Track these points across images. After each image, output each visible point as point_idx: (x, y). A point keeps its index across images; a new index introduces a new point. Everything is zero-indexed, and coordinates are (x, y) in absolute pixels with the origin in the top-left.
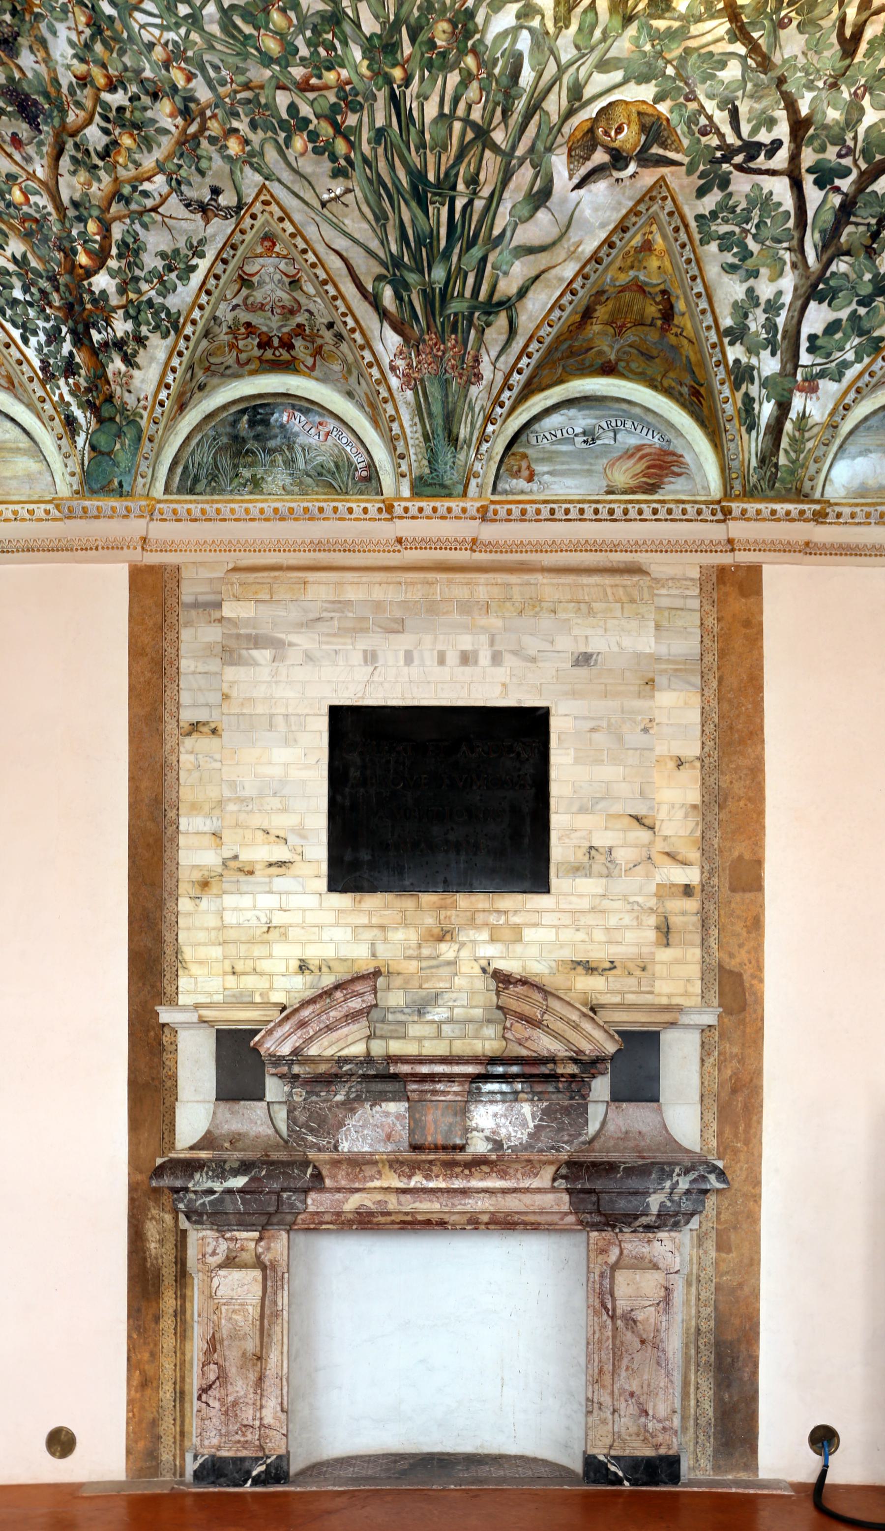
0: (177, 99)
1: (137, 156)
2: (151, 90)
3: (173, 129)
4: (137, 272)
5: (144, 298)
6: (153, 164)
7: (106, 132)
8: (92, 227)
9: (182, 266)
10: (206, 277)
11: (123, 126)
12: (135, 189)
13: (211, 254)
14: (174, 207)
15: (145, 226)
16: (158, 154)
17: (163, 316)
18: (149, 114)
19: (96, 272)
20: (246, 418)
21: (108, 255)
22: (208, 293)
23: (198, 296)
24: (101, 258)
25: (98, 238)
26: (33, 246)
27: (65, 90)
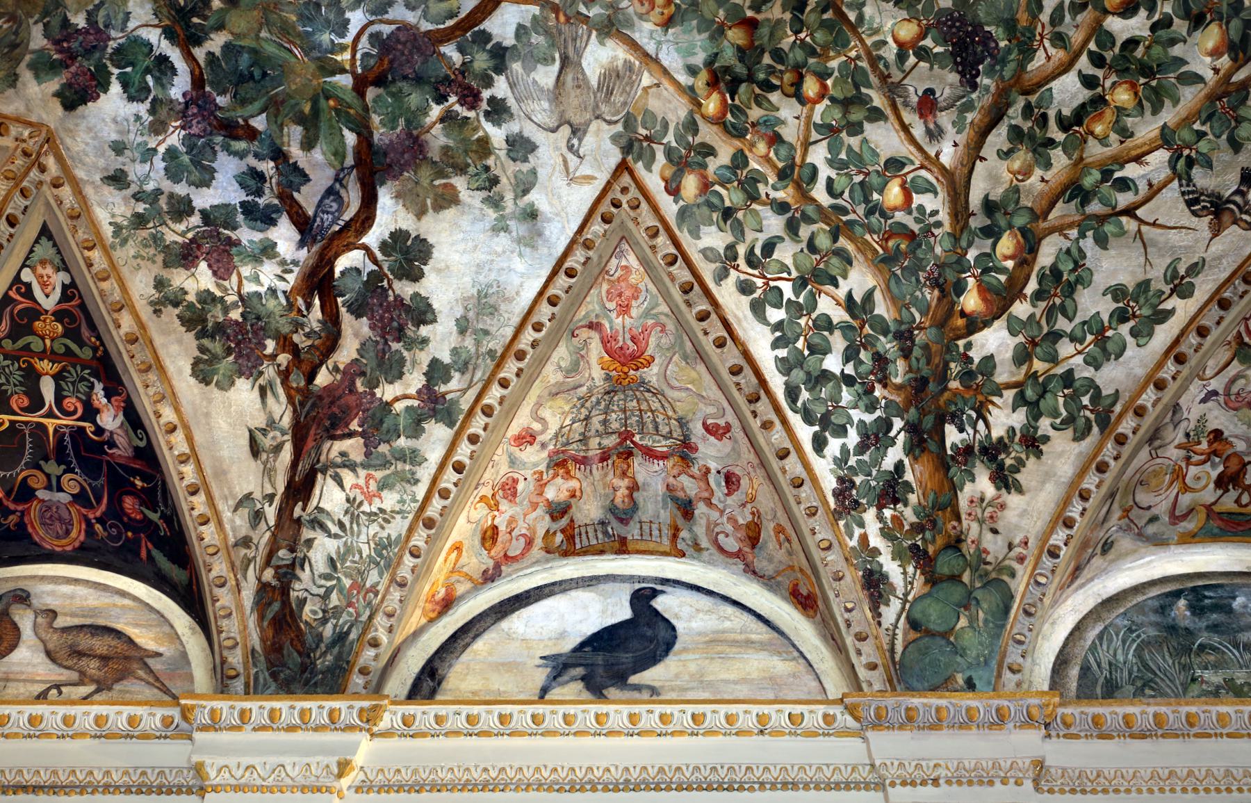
0: (1235, 24)
1: (1129, 121)
2: (1195, 10)
3: (1209, 75)
4: (1062, 324)
5: (1059, 370)
6: (1157, 132)
7: (1088, 82)
8: (1006, 244)
9: (1146, 311)
10: (1183, 333)
11: (1120, 73)
12: (1106, 174)
13: (1204, 287)
14: (1169, 206)
15: (1102, 242)
16: (1168, 116)
17: (1086, 400)
18: (1177, 50)
19: (987, 324)
20: (1182, 603)
21: (1020, 295)
22: (1180, 360)
23: (1160, 365)
24: (1000, 301)
25: (1010, 264)
26: (890, 283)
27: (1045, 17)
